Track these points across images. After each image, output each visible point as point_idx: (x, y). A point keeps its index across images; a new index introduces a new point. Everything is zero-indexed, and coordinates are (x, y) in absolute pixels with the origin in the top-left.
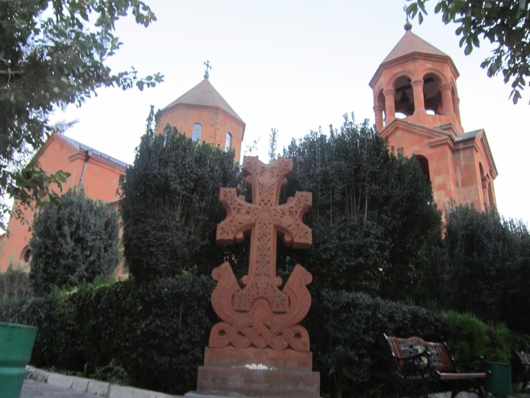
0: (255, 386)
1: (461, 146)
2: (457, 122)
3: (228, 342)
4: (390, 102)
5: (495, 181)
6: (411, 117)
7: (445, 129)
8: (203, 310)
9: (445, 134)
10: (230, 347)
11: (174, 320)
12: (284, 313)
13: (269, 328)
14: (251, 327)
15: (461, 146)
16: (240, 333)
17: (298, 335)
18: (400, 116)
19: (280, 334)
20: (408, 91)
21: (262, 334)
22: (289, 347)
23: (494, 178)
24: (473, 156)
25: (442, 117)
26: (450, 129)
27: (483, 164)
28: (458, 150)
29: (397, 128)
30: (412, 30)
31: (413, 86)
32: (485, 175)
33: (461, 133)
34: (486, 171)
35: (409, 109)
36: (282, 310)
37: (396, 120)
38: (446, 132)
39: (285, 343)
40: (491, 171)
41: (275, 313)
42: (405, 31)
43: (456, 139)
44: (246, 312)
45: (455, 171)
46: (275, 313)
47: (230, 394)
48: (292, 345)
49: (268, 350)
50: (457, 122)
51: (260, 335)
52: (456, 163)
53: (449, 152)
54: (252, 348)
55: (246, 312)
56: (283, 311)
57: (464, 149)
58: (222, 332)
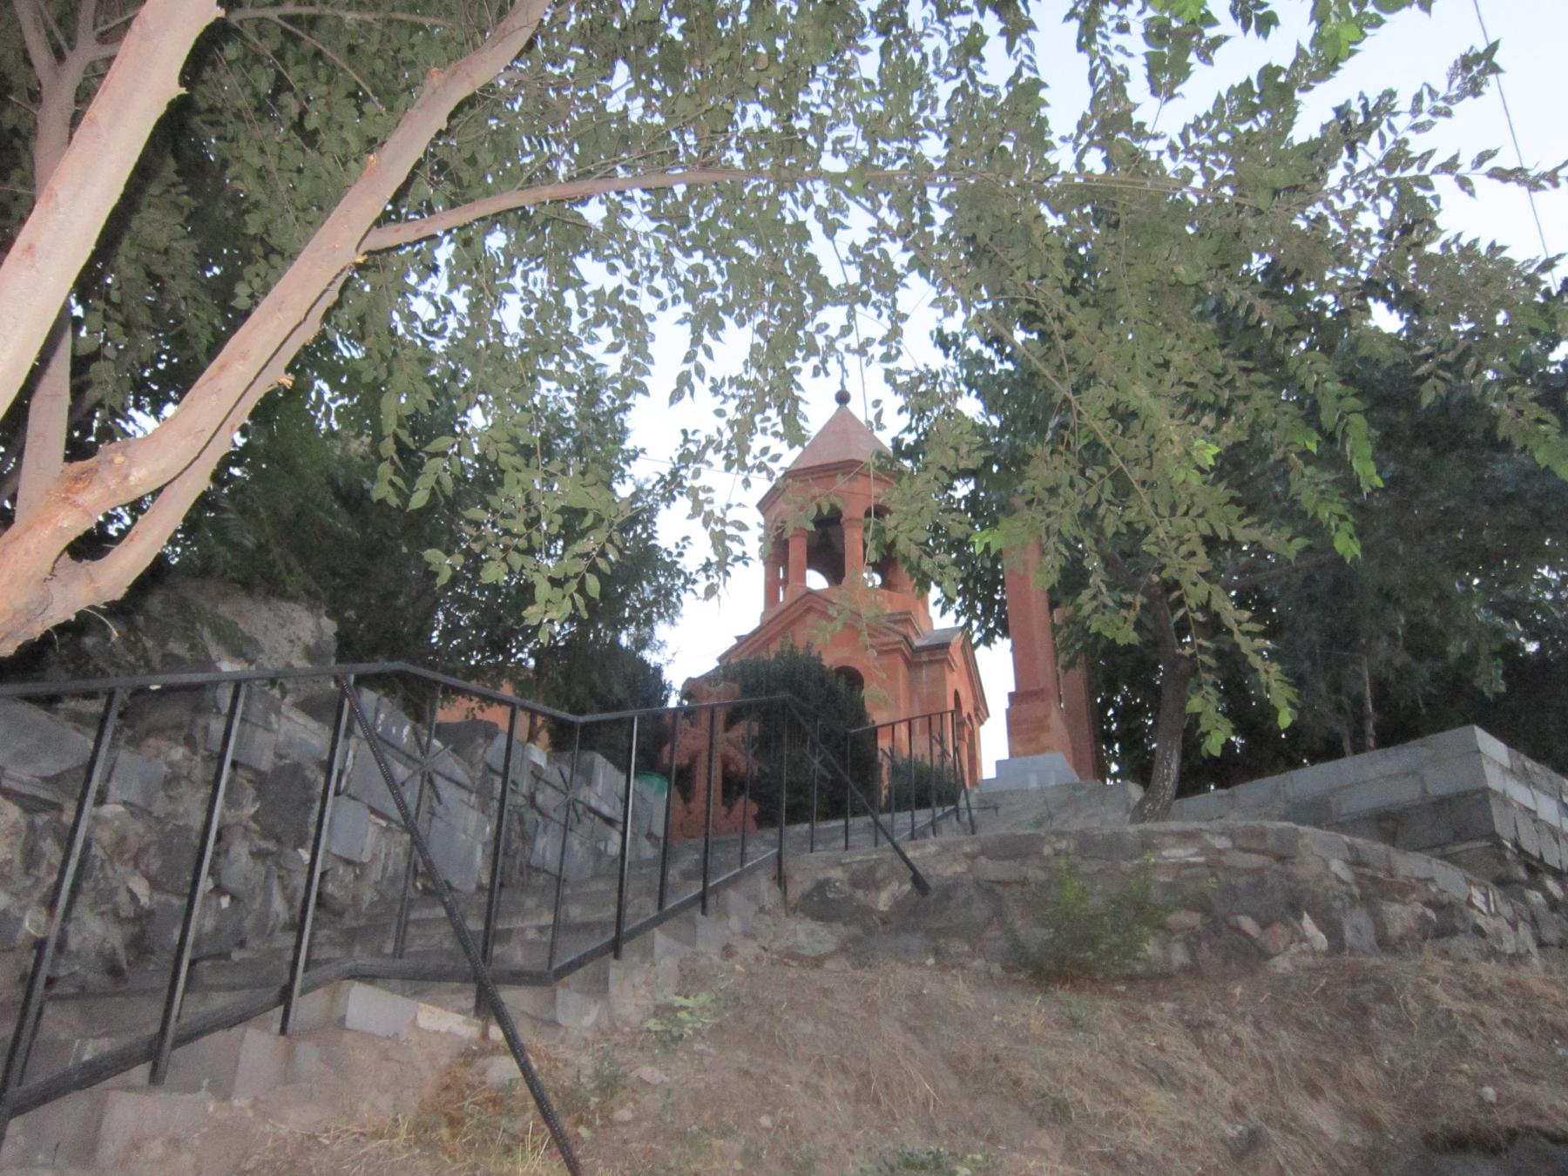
1: (925, 657)
2: (920, 607)
4: (798, 552)
5: (982, 728)
6: (835, 589)
7: (895, 622)
9: (898, 633)
15: (925, 657)
18: (816, 581)
20: (831, 530)
23: (981, 723)
24: (944, 679)
25: (895, 595)
26: (908, 621)
27: (962, 694)
28: (919, 665)
29: (809, 610)
30: (849, 405)
31: (845, 526)
32: (965, 715)
33: (926, 629)
34: (967, 708)
35: (835, 571)
37: (810, 592)
38: (896, 627)
40: (976, 709)
42: (837, 406)
43: (918, 643)
45: (911, 701)
50: (920, 607)
52: (912, 686)
53: (902, 668)
57: (931, 662)
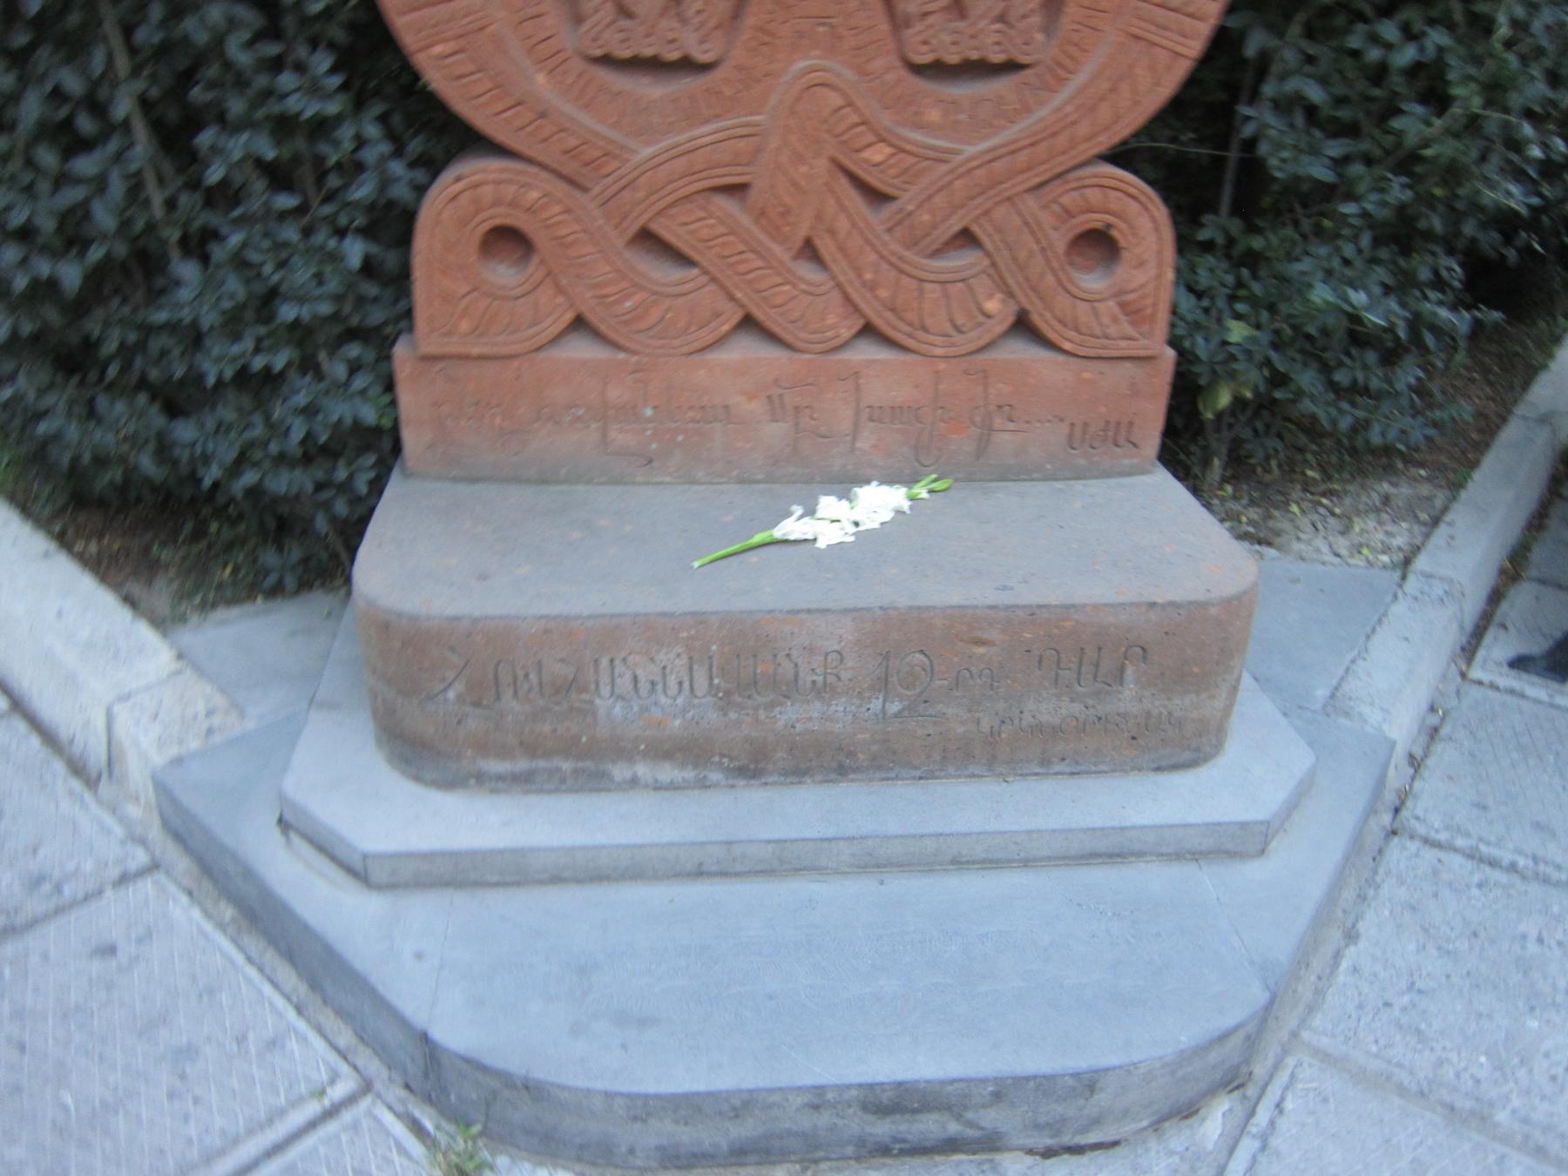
0: (796, 716)
3: (569, 316)
8: (322, 62)
10: (580, 350)
11: (85, 165)
12: (1011, 67)
13: (876, 196)
14: (736, 190)
16: (647, 238)
17: (1099, 244)
19: (966, 238)
21: (825, 246)
22: (1023, 326)
36: (991, 45)
39: (992, 306)
41: (938, 70)
44: (687, 65)
46: (938, 70)
47: (620, 771)
48: (1035, 318)
49: (867, 352)
51: (809, 251)
54: (747, 349)
55: (687, 65)
56: (997, 57)
58: (507, 240)
